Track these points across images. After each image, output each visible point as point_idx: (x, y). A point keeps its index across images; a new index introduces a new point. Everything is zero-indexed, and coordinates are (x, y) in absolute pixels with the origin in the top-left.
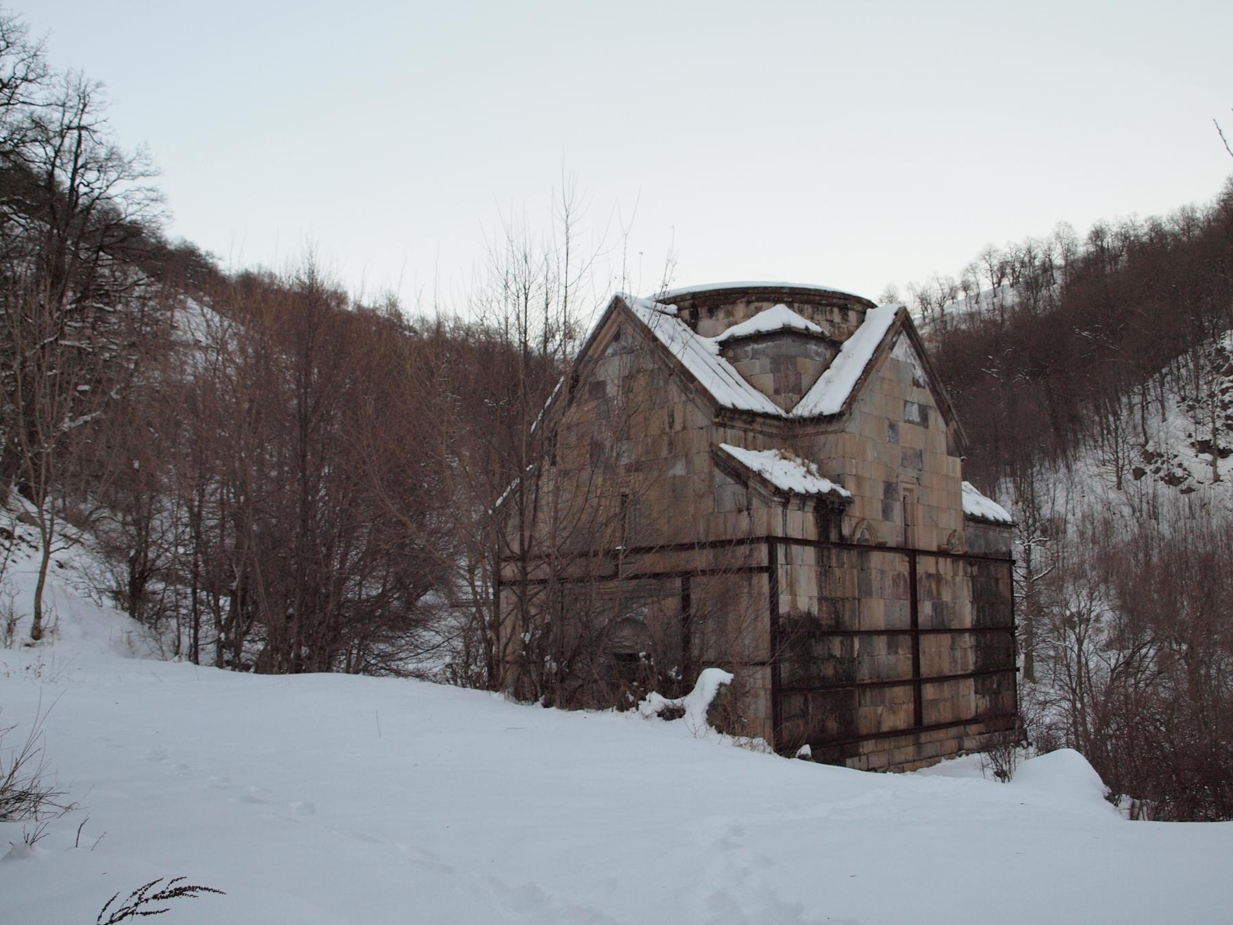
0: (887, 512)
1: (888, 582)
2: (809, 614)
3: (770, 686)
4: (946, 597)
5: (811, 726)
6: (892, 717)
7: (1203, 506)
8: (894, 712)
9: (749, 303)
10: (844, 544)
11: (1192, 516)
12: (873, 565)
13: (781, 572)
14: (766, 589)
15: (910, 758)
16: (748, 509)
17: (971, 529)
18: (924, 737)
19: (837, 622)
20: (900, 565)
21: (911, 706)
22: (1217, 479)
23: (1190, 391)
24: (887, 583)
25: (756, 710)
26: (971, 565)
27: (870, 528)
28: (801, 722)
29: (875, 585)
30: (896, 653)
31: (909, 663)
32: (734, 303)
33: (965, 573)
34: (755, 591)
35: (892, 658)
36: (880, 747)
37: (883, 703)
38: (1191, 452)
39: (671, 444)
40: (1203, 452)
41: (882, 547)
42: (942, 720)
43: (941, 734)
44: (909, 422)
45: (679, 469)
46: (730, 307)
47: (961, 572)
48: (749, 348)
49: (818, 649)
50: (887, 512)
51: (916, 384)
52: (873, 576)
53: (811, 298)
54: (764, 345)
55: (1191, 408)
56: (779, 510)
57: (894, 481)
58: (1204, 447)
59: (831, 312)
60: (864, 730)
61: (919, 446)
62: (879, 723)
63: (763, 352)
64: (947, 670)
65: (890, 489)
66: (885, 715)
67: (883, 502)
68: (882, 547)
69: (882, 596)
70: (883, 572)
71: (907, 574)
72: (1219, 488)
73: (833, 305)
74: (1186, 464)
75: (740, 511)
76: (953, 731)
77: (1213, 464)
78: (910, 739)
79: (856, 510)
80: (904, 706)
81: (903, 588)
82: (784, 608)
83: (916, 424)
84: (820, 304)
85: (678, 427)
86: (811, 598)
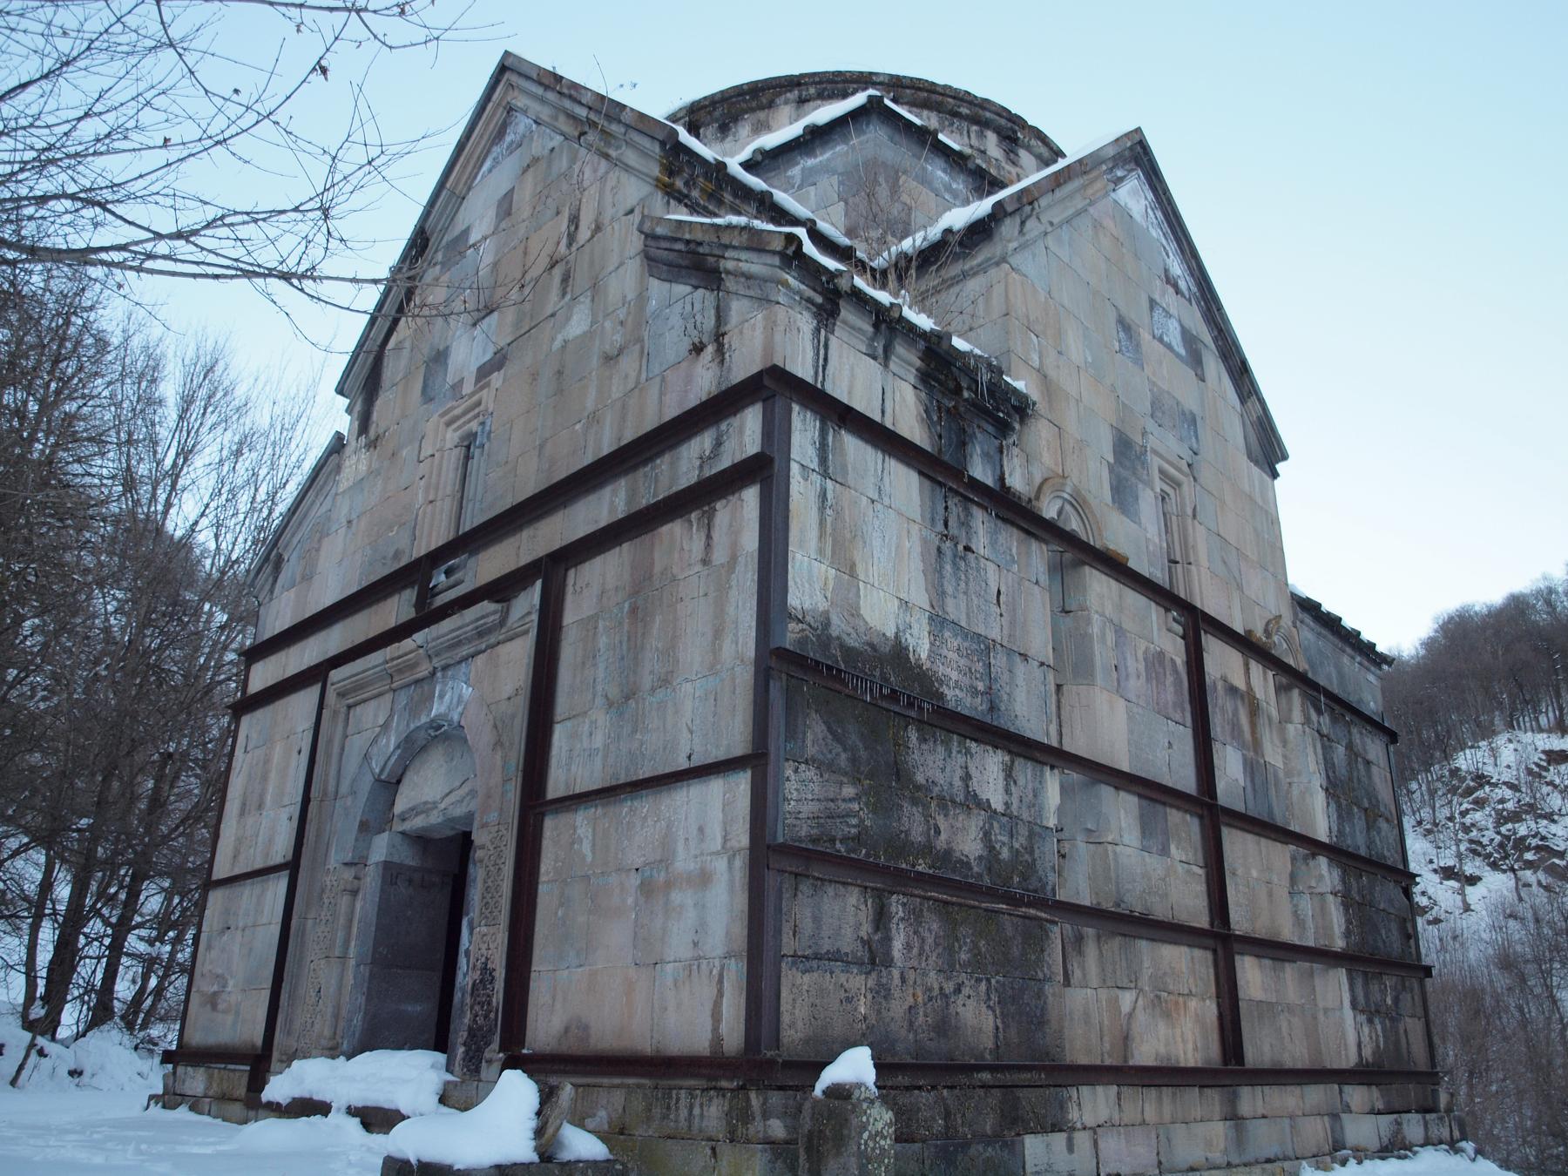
0: (1123, 496)
1: (1135, 665)
2: (899, 653)
3: (744, 840)
4: (1273, 755)
5: (897, 1008)
6: (1162, 1028)
7: (1455, 938)
8: (1167, 1015)
9: (802, 101)
10: (1013, 510)
11: (1443, 949)
12: (1093, 600)
13: (802, 491)
14: (750, 541)
15: (1217, 1157)
16: (719, 337)
17: (1308, 634)
18: (1251, 1100)
19: (993, 708)
20: (1162, 634)
21: (1211, 1009)
22: (1467, 908)
23: (1425, 813)
24: (1131, 663)
25: (701, 928)
26: (1319, 712)
27: (1078, 503)
28: (857, 981)
29: (1102, 655)
30: (1164, 851)
31: (1200, 888)
32: (771, 105)
33: (1307, 721)
34: (719, 556)
35: (1154, 863)
36: (1130, 1113)
37: (1134, 983)
38: (1436, 878)
39: (566, 279)
40: (1448, 878)
41: (1115, 566)
42: (1289, 1063)
43: (1288, 1098)
44: (1161, 340)
45: (578, 324)
46: (761, 115)
47: (1297, 715)
48: (795, 172)
49: (934, 763)
50: (1123, 496)
51: (1171, 281)
52: (1095, 629)
53: (934, 97)
54: (828, 155)
55: (1429, 832)
56: (805, 322)
57: (1138, 439)
58: (1448, 873)
59: (981, 135)
60: (1081, 1048)
61: (1191, 403)
62: (1126, 1039)
63: (826, 169)
64: (1288, 934)
65: (1126, 451)
66: (1141, 1017)
67: (1111, 470)
68: (1115, 566)
69: (1119, 690)
70: (1119, 631)
71: (1180, 660)
72: (1472, 918)
73: (984, 124)
74: (1430, 891)
75: (698, 349)
76: (1316, 1095)
77: (1462, 893)
78: (1214, 1096)
79: (1039, 434)
80: (1193, 1003)
81: (1174, 691)
82: (809, 584)
83: (1178, 355)
84: (955, 114)
85: (584, 234)
86: (904, 604)
